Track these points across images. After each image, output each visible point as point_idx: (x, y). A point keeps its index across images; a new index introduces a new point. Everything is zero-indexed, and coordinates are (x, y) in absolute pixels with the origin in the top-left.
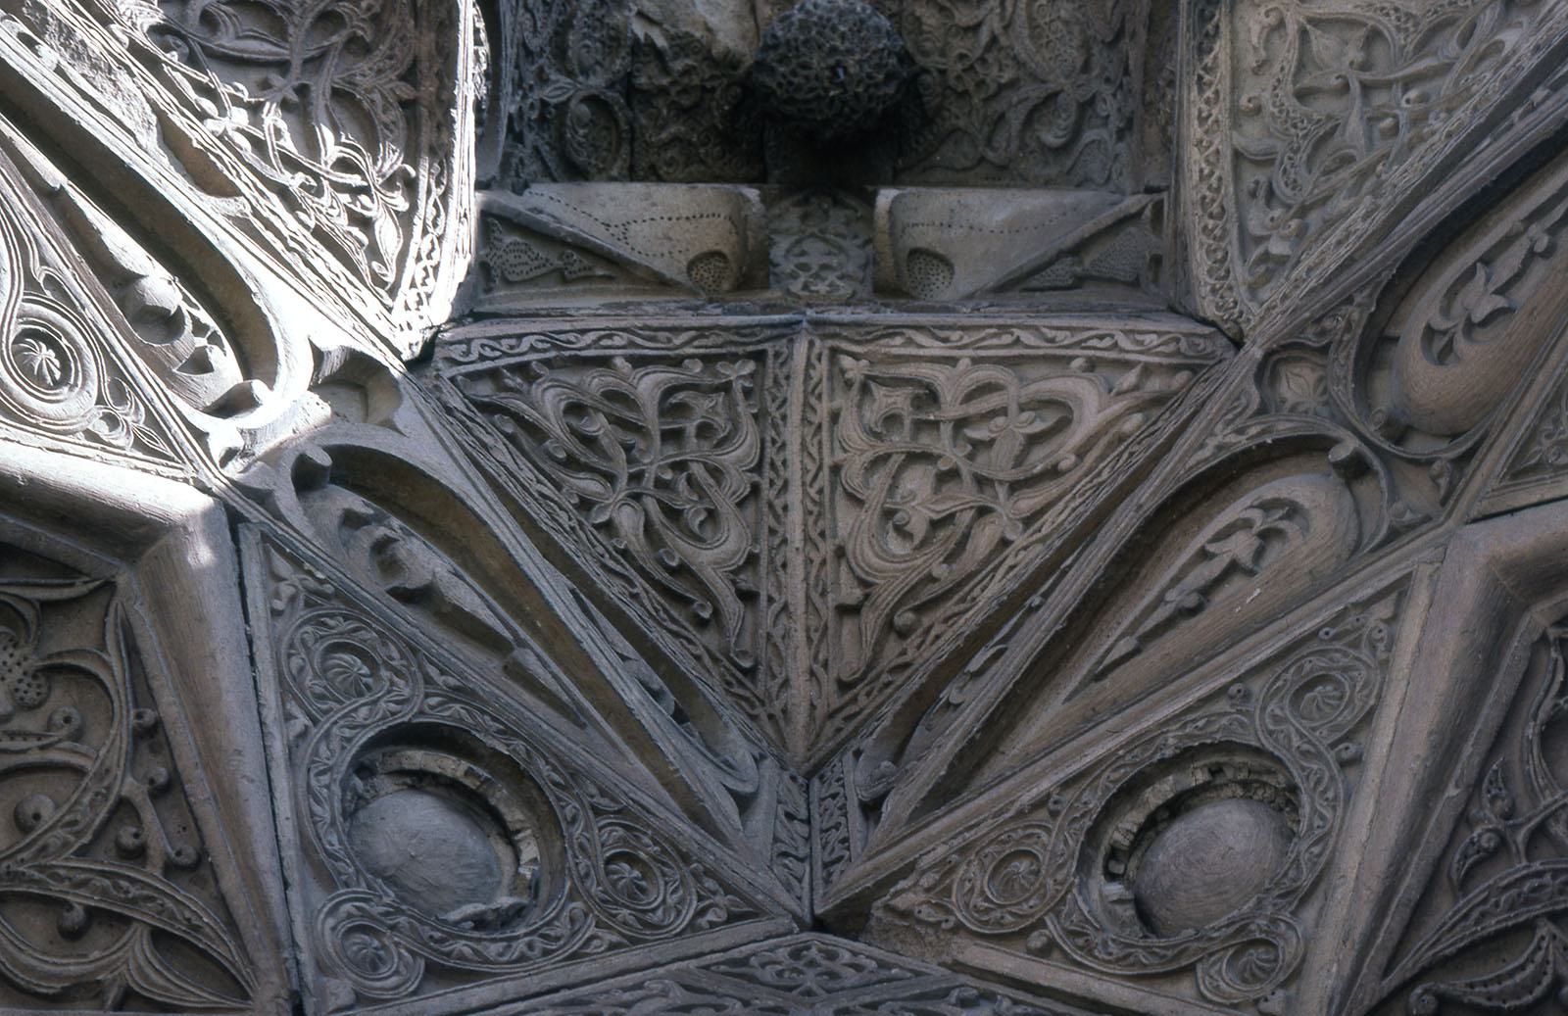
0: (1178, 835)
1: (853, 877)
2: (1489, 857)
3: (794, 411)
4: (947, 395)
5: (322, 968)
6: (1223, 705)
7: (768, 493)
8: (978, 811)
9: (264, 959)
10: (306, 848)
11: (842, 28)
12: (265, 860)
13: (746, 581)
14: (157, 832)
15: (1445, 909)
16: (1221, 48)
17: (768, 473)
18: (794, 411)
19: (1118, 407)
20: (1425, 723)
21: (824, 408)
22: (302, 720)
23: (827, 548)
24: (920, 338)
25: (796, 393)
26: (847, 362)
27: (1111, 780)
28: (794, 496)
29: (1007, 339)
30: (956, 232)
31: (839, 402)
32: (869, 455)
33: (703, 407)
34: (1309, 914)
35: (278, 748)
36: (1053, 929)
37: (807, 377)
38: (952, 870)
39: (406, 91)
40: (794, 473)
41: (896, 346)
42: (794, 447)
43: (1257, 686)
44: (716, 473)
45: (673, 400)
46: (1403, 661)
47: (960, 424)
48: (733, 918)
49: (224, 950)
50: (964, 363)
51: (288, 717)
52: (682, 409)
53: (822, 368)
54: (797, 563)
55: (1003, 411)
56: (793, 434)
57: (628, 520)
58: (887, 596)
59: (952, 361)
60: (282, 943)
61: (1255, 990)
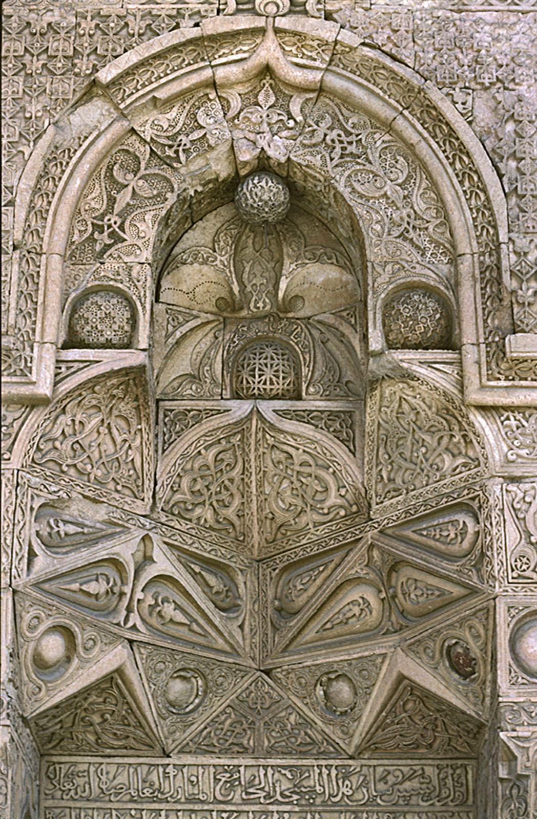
0: (334, 683)
1: (269, 663)
2: (389, 725)
3: (253, 448)
4: (296, 460)
5: (166, 738)
6: (345, 664)
7: (246, 480)
8: (295, 660)
9: (157, 743)
10: (159, 714)
11: (267, 210)
12: (153, 726)
13: (240, 513)
14: (132, 720)
15: (380, 732)
16: (377, 392)
17: (246, 473)
18: (253, 448)
19: (339, 501)
20: (381, 700)
21: (261, 450)
22: (153, 687)
23: (263, 497)
24: (289, 438)
25: (252, 441)
26: (268, 436)
27: (324, 670)
28: (253, 478)
29: (313, 446)
30: (306, 285)
31: (265, 451)
32: (273, 473)
33: (228, 457)
34: (356, 723)
35: (150, 697)
36: (308, 700)
37: (256, 436)
38: (289, 673)
39: (135, 404)
40: (253, 470)
41: (281, 437)
42: (253, 463)
43: (353, 662)
44: (231, 480)
45: (218, 459)
46: (381, 676)
47: (298, 472)
48: (242, 677)
49: (148, 741)
50: (301, 451)
51: (150, 687)
52: (222, 460)
53: (260, 435)
54: (255, 502)
55: (310, 475)
56: (252, 457)
57: (209, 515)
58: (279, 521)
59: (298, 449)
60: (159, 740)
61: (345, 737)
